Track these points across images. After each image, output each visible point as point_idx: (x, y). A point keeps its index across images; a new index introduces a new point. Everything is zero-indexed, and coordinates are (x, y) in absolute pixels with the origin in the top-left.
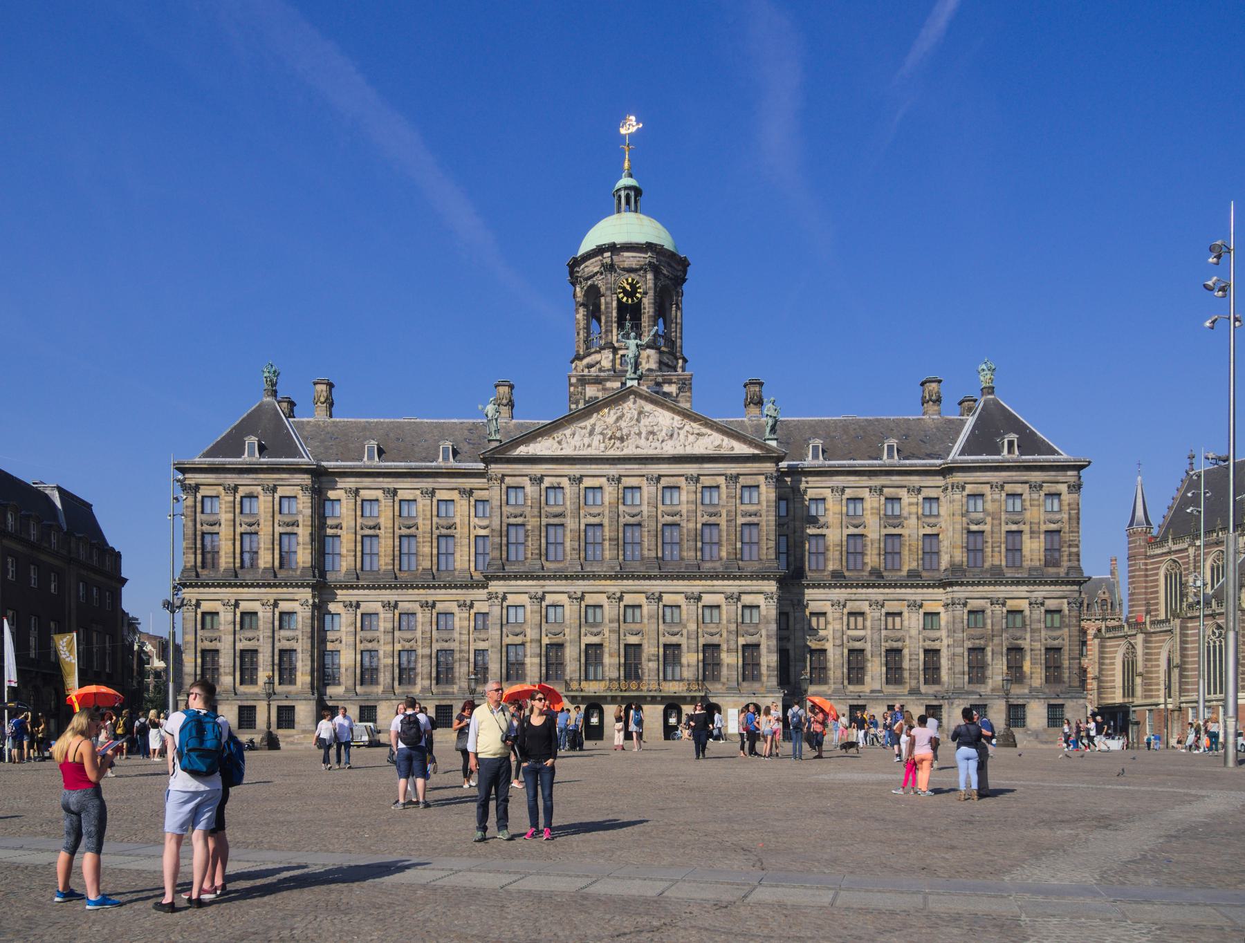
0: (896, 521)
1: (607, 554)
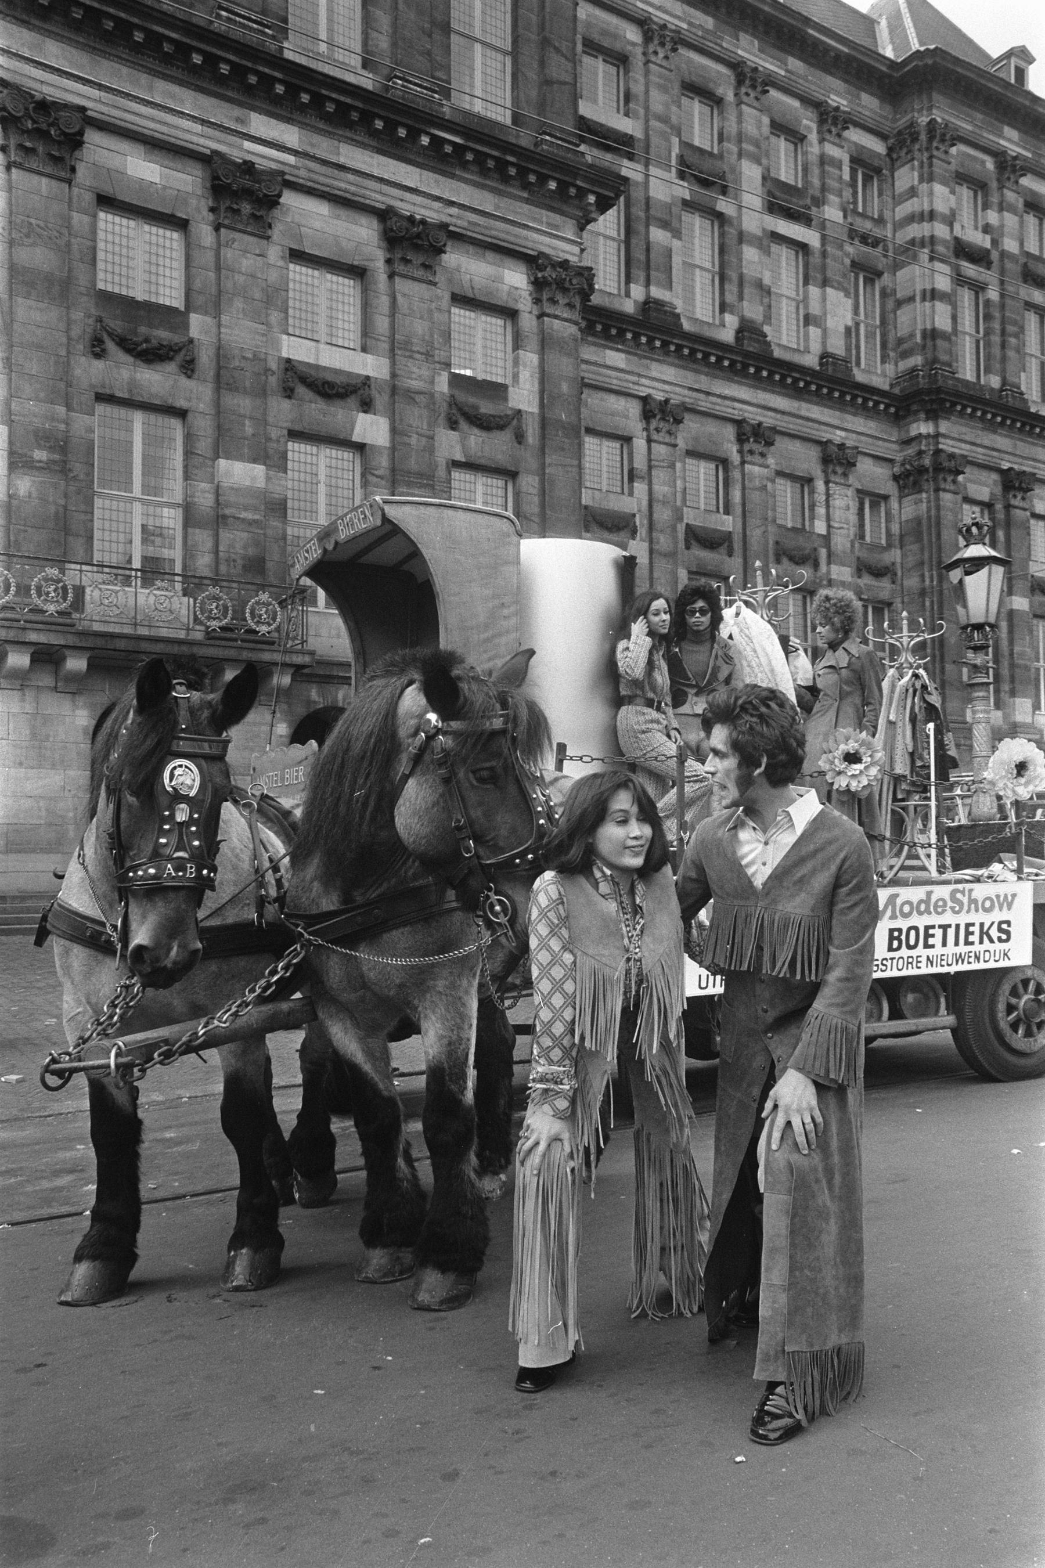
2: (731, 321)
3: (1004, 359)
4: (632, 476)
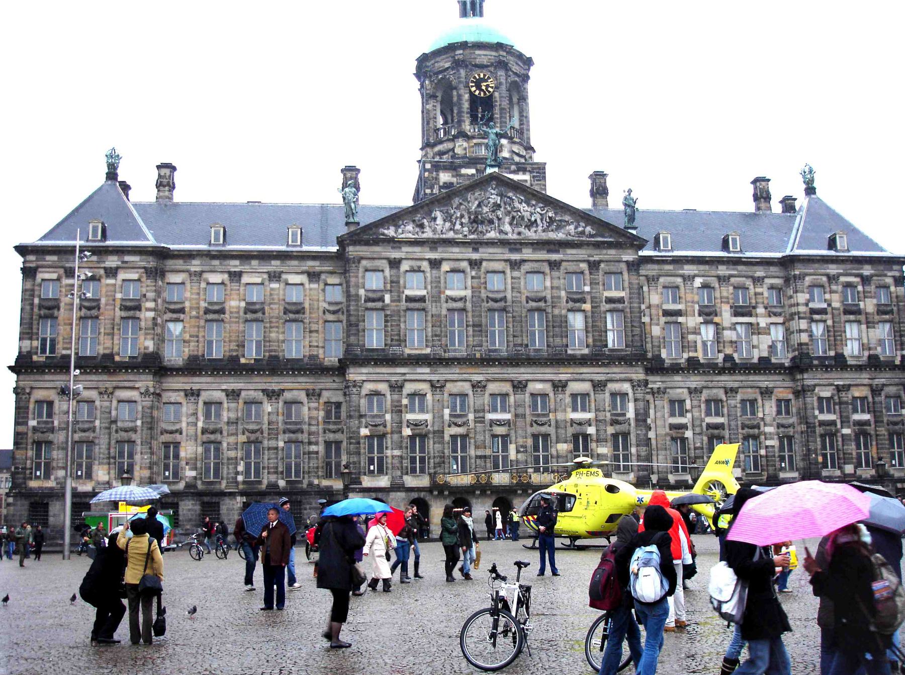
0: (744, 310)
1: (471, 339)
2: (721, 356)
3: (835, 345)
4: (687, 411)
